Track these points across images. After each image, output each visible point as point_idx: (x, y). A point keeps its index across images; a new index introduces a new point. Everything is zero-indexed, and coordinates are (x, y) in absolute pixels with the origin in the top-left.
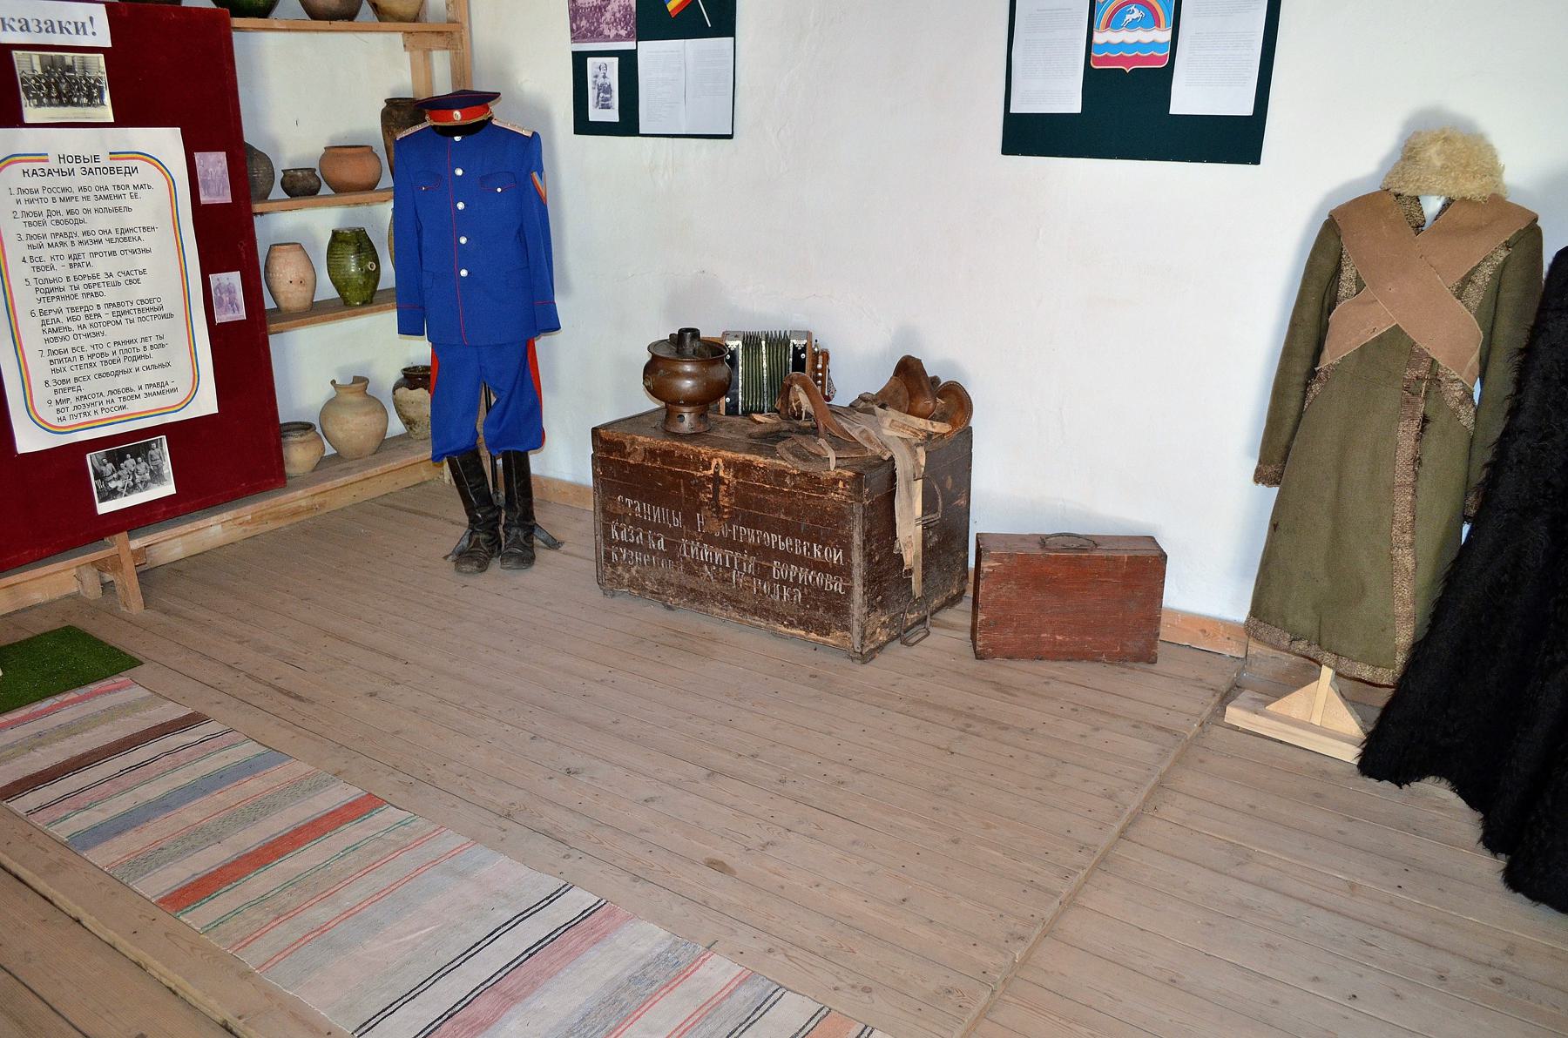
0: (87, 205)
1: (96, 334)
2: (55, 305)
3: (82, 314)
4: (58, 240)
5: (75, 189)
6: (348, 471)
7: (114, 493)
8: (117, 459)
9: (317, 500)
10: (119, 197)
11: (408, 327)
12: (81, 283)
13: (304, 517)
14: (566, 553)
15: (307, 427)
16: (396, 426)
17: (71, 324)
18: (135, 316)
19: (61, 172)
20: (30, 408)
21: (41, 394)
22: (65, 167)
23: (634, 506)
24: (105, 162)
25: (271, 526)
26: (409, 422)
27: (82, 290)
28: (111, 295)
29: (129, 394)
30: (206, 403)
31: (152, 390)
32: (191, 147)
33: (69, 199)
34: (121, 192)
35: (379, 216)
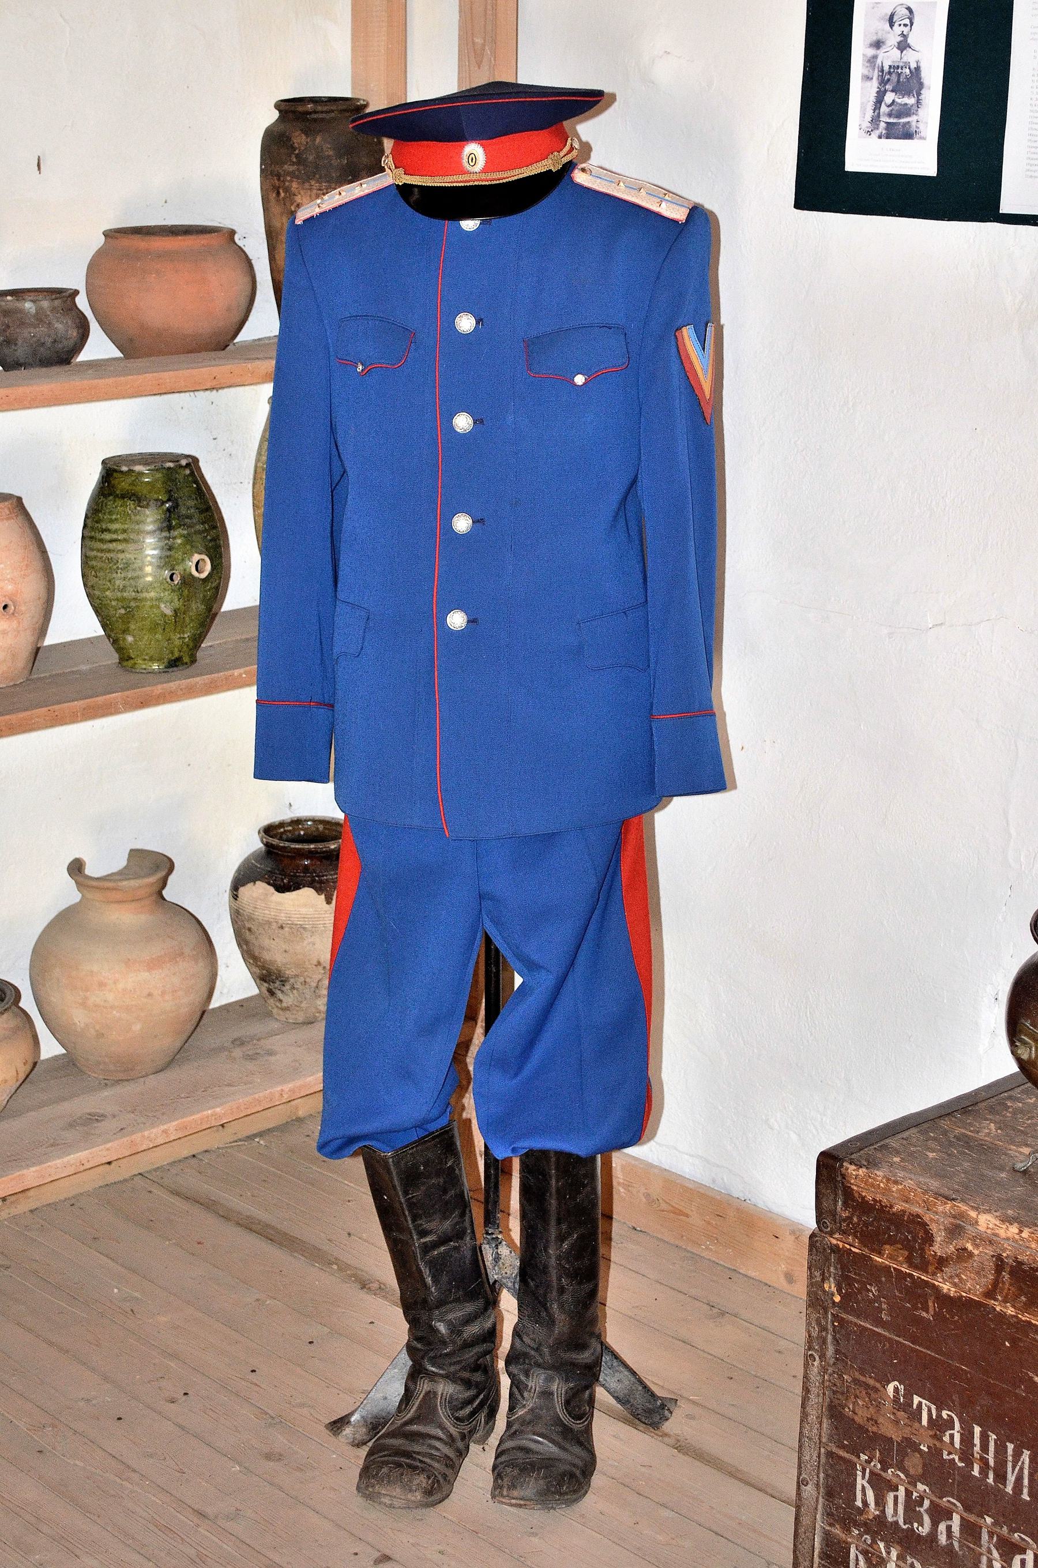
11: (278, 756)
14: (681, 1447)
16: (235, 981)
23: (939, 1426)
26: (269, 977)
35: (225, 430)
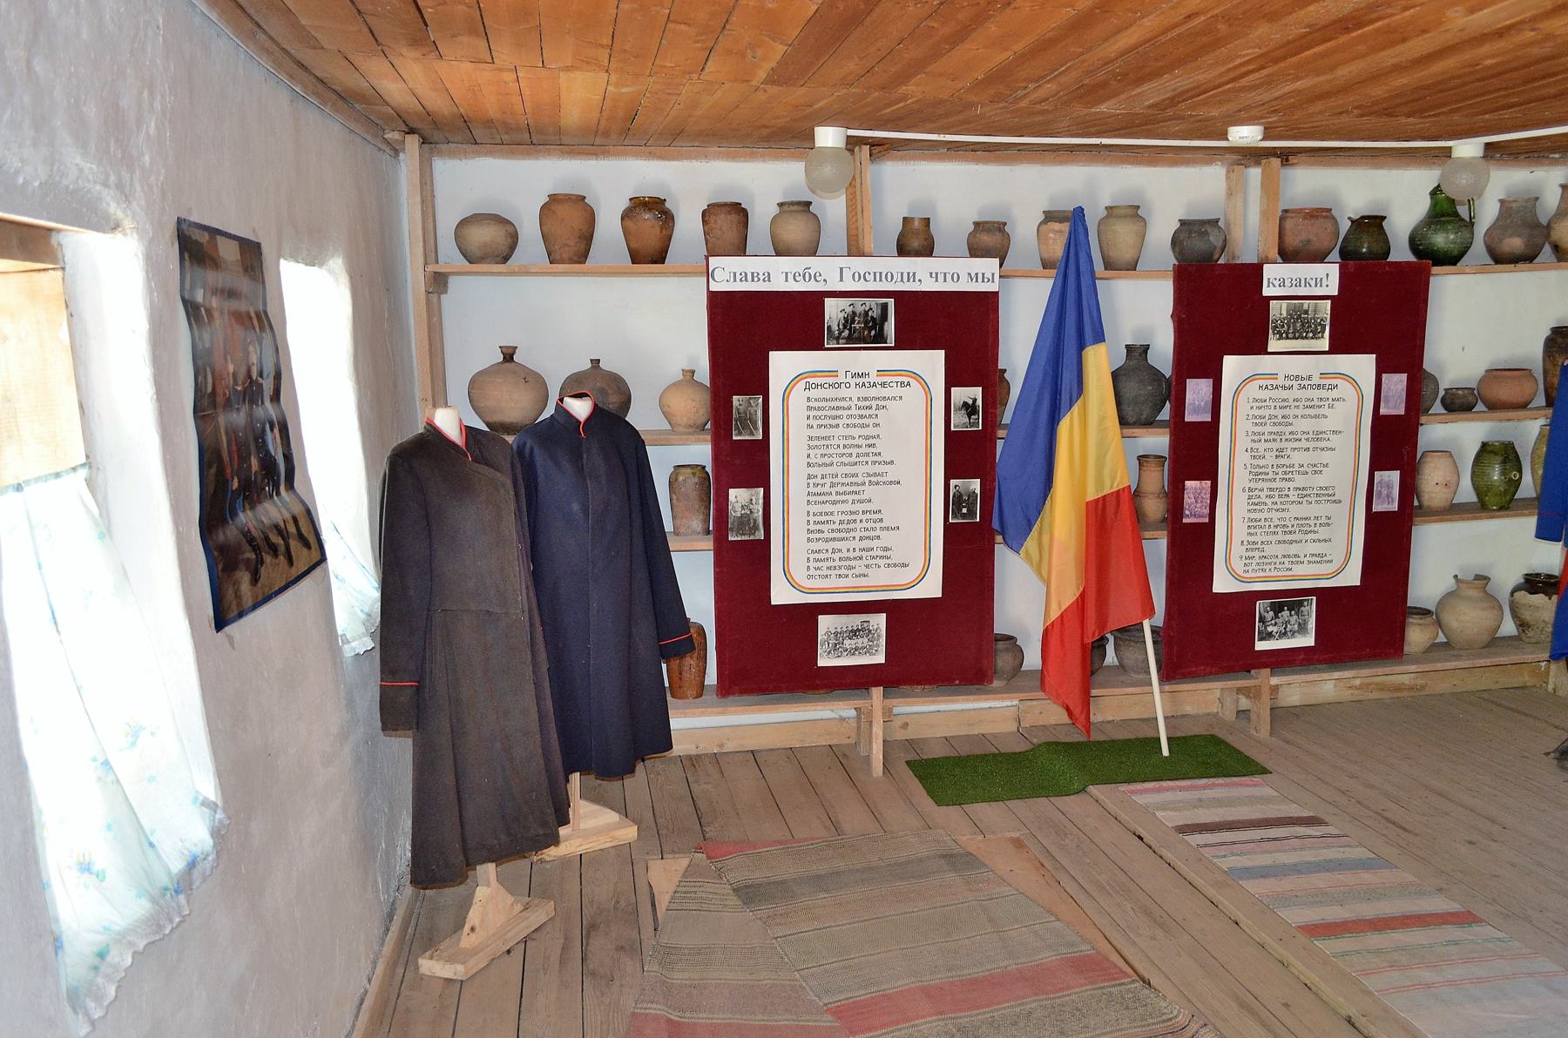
2: (1260, 485)
6: (1458, 658)
7: (1269, 636)
8: (1277, 609)
9: (1420, 682)
11: (1544, 533)
13: (1406, 694)
15: (1425, 612)
16: (1508, 627)
17: (1269, 501)
19: (1284, 388)
20: (1227, 560)
21: (1237, 550)
24: (1316, 380)
25: (1375, 695)
26: (1523, 625)
28: (1300, 481)
29: (1296, 559)
30: (1352, 576)
32: (1381, 370)
35: (1529, 431)
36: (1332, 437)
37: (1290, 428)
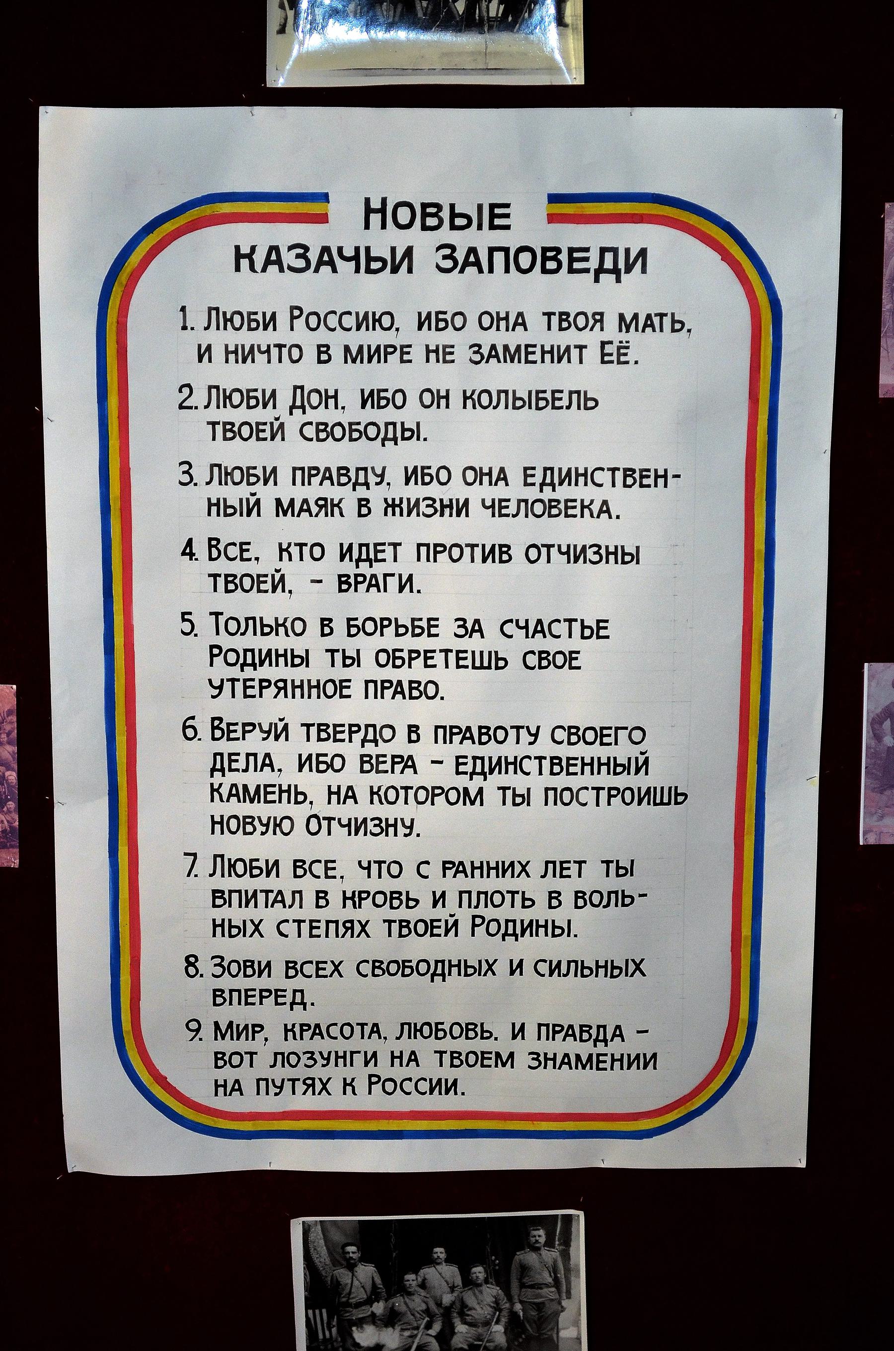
0: (442, 377)
1: (386, 827)
2: (268, 708)
3: (352, 750)
4: (314, 491)
5: (406, 321)
8: (397, 1255)
10: (560, 355)
12: (368, 645)
17: (314, 784)
18: (536, 782)
21: (168, 997)
22: (383, 239)
24: (529, 227)
27: (369, 669)
28: (464, 696)
29: (474, 1044)
31: (560, 1046)
33: (379, 354)
34: (571, 337)
36: (620, 498)
37: (409, 454)
